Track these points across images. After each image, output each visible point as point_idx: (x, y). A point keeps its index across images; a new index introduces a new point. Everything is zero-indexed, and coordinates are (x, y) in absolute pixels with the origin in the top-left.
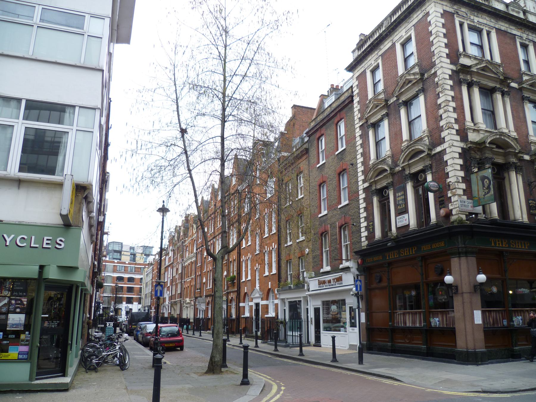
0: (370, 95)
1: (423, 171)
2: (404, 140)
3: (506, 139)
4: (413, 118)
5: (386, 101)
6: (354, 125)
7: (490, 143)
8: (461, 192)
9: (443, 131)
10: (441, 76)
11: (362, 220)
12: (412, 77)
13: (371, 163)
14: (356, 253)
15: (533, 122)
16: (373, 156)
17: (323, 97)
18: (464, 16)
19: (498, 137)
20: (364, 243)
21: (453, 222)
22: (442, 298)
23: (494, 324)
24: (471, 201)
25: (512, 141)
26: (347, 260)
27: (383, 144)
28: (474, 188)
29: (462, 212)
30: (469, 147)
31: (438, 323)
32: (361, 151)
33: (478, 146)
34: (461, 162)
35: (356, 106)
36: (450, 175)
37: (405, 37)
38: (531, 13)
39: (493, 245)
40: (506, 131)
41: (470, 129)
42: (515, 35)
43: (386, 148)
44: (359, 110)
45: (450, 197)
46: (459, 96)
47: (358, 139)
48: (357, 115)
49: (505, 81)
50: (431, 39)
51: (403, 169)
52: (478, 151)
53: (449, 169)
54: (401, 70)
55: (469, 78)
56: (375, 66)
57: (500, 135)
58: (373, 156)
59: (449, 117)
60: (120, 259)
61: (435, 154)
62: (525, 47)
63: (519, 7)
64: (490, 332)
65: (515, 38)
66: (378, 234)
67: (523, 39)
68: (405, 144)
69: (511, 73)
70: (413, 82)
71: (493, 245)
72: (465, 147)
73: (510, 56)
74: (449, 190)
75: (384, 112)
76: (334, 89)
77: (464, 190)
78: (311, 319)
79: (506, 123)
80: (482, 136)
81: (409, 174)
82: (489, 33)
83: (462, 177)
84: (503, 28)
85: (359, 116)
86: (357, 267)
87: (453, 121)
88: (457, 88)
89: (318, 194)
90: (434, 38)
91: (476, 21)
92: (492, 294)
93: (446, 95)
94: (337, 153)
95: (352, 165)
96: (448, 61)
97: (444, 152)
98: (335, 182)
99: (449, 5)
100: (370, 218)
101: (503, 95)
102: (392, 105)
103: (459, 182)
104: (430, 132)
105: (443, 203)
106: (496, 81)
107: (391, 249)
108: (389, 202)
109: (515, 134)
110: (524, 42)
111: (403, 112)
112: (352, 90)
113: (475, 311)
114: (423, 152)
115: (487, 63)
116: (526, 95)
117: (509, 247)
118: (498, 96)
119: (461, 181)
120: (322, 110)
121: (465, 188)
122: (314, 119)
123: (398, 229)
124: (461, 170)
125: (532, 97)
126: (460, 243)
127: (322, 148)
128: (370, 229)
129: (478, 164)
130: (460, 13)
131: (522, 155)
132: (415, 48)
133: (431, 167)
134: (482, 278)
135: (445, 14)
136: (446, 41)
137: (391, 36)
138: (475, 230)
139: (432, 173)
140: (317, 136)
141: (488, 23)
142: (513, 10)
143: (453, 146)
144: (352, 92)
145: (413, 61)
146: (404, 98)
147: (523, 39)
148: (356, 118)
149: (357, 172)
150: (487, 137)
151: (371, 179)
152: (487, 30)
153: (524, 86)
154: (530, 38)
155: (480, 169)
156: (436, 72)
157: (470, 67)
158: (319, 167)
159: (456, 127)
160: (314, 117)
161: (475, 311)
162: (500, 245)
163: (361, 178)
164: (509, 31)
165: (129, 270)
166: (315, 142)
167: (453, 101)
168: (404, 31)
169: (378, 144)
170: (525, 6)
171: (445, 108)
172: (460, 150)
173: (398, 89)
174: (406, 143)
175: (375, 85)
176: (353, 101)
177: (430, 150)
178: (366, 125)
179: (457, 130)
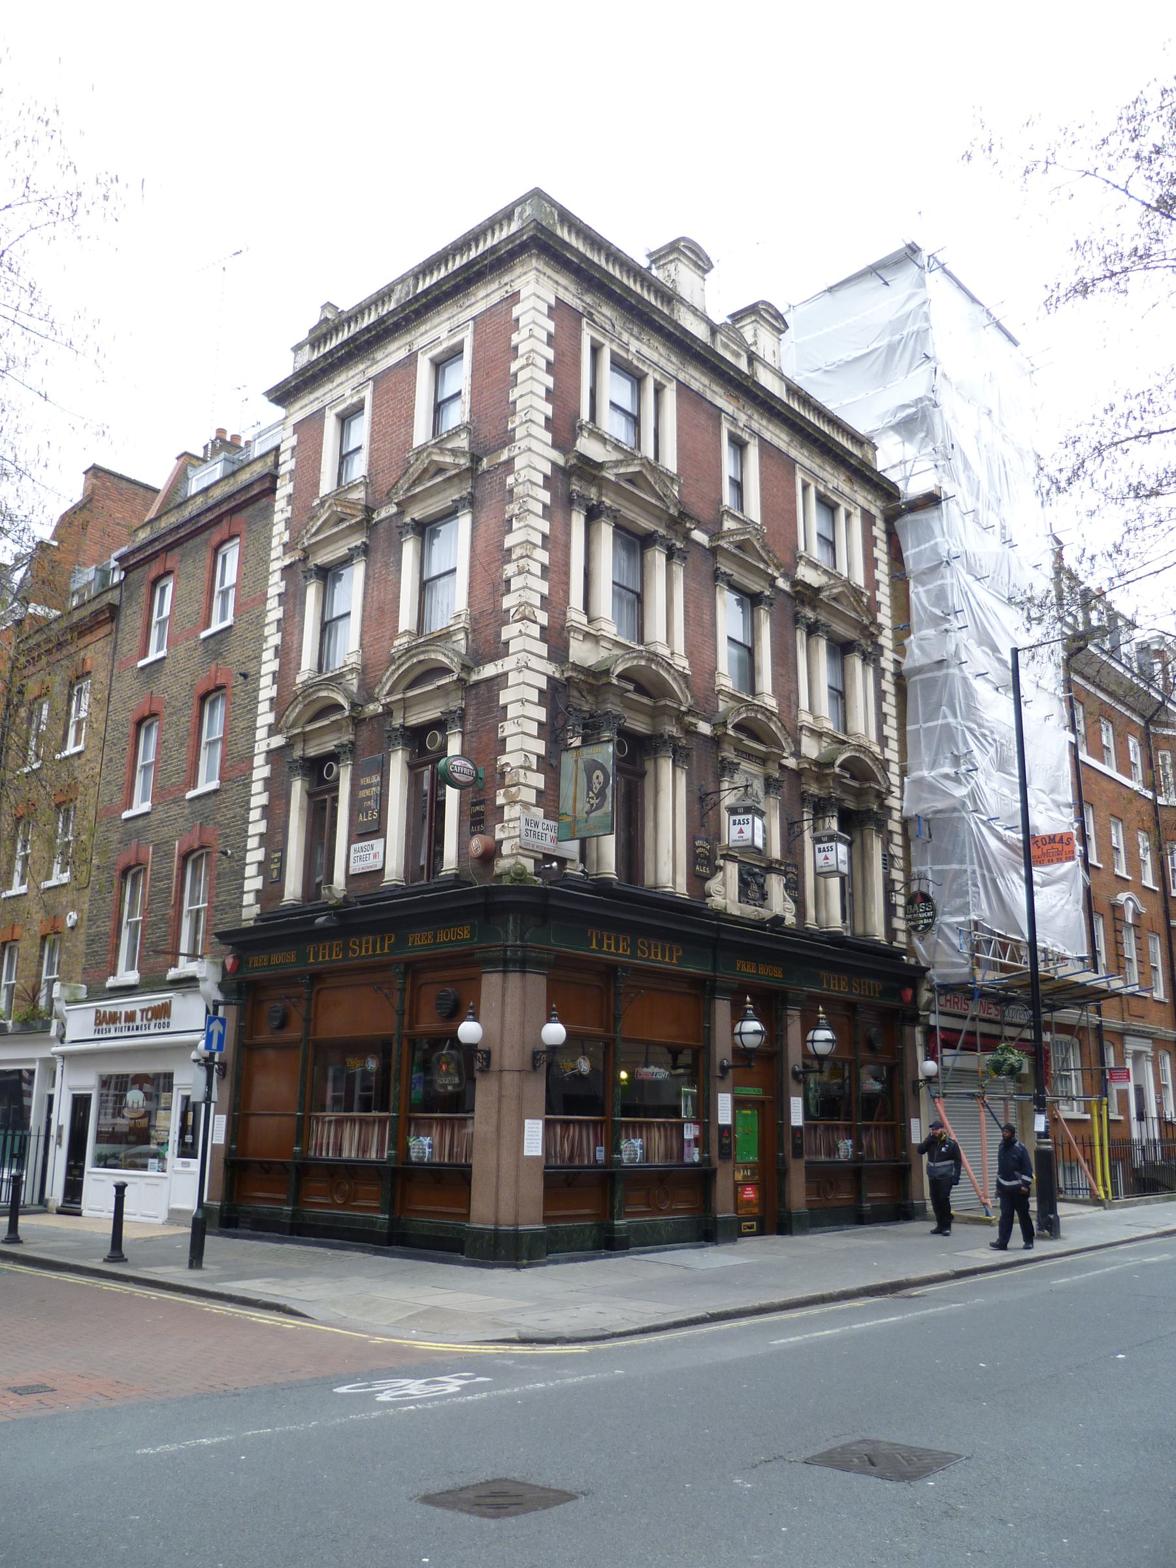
0: (327, 485)
1: (440, 725)
2: (401, 630)
3: (661, 672)
4: (434, 573)
5: (369, 510)
6: (265, 562)
7: (619, 676)
8: (530, 796)
9: (506, 623)
10: (524, 475)
11: (252, 843)
12: (448, 459)
13: (300, 679)
14: (222, 936)
15: (730, 638)
16: (308, 660)
17: (188, 461)
18: (608, 327)
19: (643, 663)
20: (250, 909)
21: (500, 876)
22: (447, 1082)
24: (552, 823)
25: (675, 679)
26: (193, 956)
27: (341, 633)
28: (567, 788)
29: (525, 851)
30: (568, 679)
32: (275, 640)
33: (591, 680)
34: (541, 714)
35: (281, 509)
36: (510, 745)
37: (445, 345)
38: (766, 365)
39: (594, 946)
40: (664, 651)
41: (577, 630)
42: (721, 410)
43: (348, 644)
44: (287, 520)
45: (502, 807)
47: (273, 603)
48: (279, 533)
49: (679, 521)
50: (514, 366)
51: (388, 712)
52: (589, 692)
53: (508, 729)
54: (421, 434)
55: (593, 493)
56: (353, 405)
57: (649, 660)
58: (308, 660)
59: (527, 588)
61: (478, 684)
62: (739, 445)
63: (741, 341)
64: (560, 1180)
65: (720, 416)
66: (293, 888)
67: (737, 426)
68: (401, 642)
69: (698, 507)
70: (449, 474)
71: (594, 946)
72: (557, 675)
73: (699, 460)
74: (502, 786)
75: (357, 540)
76: (224, 444)
77: (539, 792)
78: (60, 1128)
79: (668, 633)
80: (604, 654)
81: (402, 726)
82: (659, 390)
83: (539, 756)
84: (695, 386)
85: (286, 537)
86: (220, 980)
87: (537, 601)
88: (559, 515)
89: (129, 749)
90: (522, 368)
91: (633, 349)
92: (580, 1077)
93: (529, 530)
94: (204, 635)
95: (245, 676)
96: (548, 437)
97: (499, 681)
98: (186, 720)
99: (572, 288)
100: (274, 841)
101: (669, 558)
102: (381, 527)
103: (528, 768)
104: (473, 619)
105: (481, 822)
106: (659, 518)
107: (323, 934)
108: (335, 800)
109: (685, 663)
110: (739, 432)
111: (409, 550)
112: (277, 457)
114: (446, 671)
115: (643, 465)
116: (723, 569)
117: (633, 955)
118: (658, 558)
119: (535, 767)
120: (179, 500)
121: (542, 786)
122: (151, 521)
123: (350, 878)
124: (539, 737)
125: (736, 577)
126: (510, 935)
127: (160, 612)
128: (273, 871)
129: (585, 727)
130: (597, 317)
131: (694, 720)
132: (469, 381)
133: (462, 716)
134: (555, 1032)
135: (558, 310)
136: (549, 381)
137: (408, 331)
138: (552, 902)
139: (463, 734)
140: (153, 574)
141: (663, 362)
142: (726, 346)
143: (528, 668)
144: (277, 465)
145: (456, 415)
146: (417, 513)
147: (737, 426)
148: (275, 542)
149: (255, 701)
150: (617, 658)
151: (293, 726)
152: (655, 380)
153: (724, 543)
154: (755, 426)
155: (586, 742)
156: (511, 461)
157: (600, 466)
158: (142, 668)
159: (543, 618)
160: (151, 514)
162: (611, 948)
163: (266, 717)
164: (709, 395)
166: (144, 590)
167: (544, 547)
168: (447, 326)
169: (327, 627)
170: (755, 343)
171: (522, 562)
173: (404, 484)
174: (405, 639)
175: (344, 458)
176: (273, 490)
177: (467, 668)
178: (301, 567)
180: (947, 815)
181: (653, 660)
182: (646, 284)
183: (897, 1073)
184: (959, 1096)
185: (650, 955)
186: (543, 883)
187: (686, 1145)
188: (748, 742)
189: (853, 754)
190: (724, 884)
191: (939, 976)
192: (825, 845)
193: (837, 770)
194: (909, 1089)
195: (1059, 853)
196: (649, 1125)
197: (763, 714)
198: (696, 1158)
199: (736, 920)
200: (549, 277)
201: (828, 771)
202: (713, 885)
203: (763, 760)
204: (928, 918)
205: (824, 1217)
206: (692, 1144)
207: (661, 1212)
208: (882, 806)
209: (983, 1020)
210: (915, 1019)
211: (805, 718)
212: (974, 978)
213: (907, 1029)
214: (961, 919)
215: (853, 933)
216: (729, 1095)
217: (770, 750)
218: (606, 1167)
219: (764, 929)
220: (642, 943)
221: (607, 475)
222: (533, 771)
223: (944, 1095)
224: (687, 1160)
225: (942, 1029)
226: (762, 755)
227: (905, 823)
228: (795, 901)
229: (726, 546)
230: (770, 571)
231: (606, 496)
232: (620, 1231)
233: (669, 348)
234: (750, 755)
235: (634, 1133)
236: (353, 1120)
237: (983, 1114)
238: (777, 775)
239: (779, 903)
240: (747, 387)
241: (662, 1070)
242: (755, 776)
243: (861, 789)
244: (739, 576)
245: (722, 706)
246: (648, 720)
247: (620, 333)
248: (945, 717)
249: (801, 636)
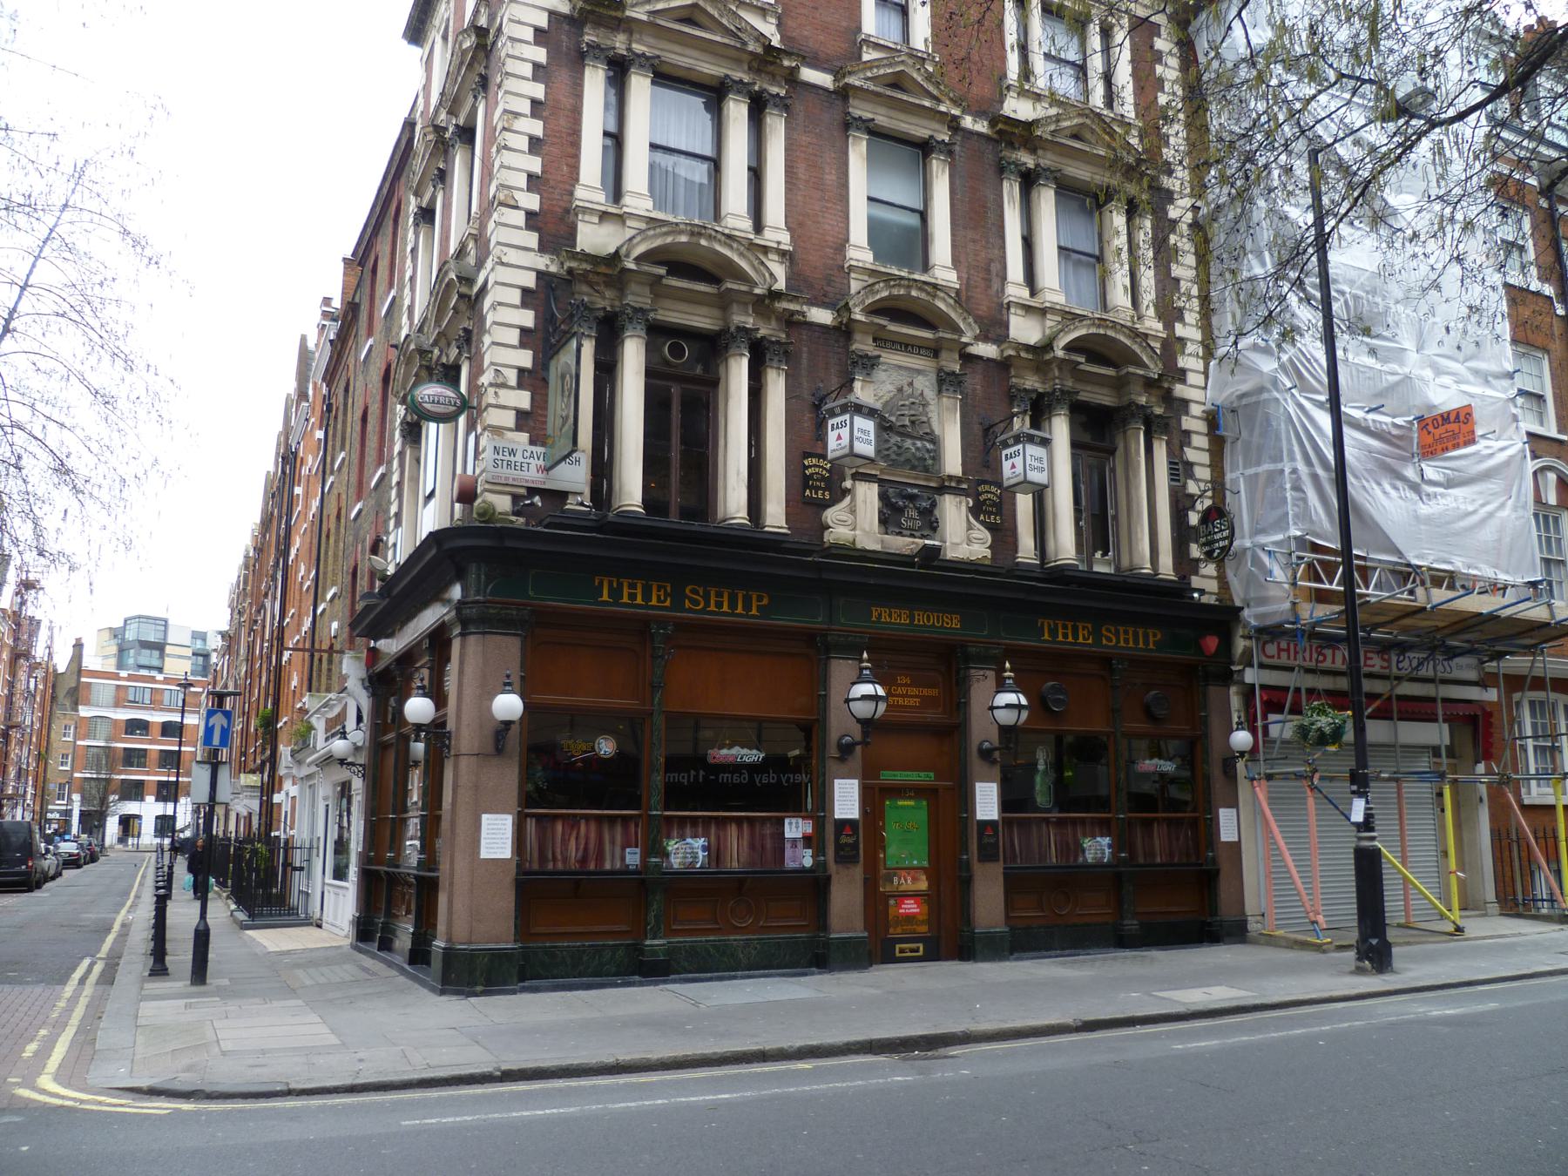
19: (684, 239)
23: (584, 860)
24: (539, 450)
25: (741, 255)
31: (701, 854)
33: (602, 269)
41: (585, 210)
46: (566, 102)
52: (607, 285)
57: (692, 234)
60: (160, 670)
64: (535, 886)
69: (812, 37)
72: (553, 269)
86: (363, 674)
88: (563, 76)
92: (597, 762)
103: (504, 386)
106: (738, 61)
113: (485, 817)
116: (857, 113)
117: (678, 605)
131: (793, 307)
143: (502, 264)
153: (854, 80)
161: (485, 817)
165: (166, 701)
172: (530, 280)
179: (530, 215)
180: (1253, 399)
181: (700, 234)
184: (1286, 776)
185: (707, 604)
186: (527, 524)
187: (788, 845)
188: (893, 327)
189: (1093, 330)
190: (853, 511)
191: (1257, 617)
192: (1012, 450)
193: (1060, 353)
194: (1216, 772)
195: (1455, 435)
196: (722, 823)
197: (920, 289)
198: (808, 862)
199: (865, 555)
201: (1048, 357)
202: (831, 515)
203: (934, 351)
204: (1223, 539)
205: (1021, 941)
206: (800, 845)
208: (1168, 398)
209: (1308, 671)
210: (1227, 677)
211: (1016, 289)
214: (1280, 537)
215: (1118, 568)
216: (856, 782)
219: (912, 565)
220: (692, 591)
222: (512, 388)
223: (1269, 777)
224: (790, 864)
225: (1263, 687)
227: (1212, 420)
228: (991, 527)
229: (857, 83)
230: (943, 108)
231: (638, 42)
232: (654, 953)
234: (906, 346)
237: (1311, 801)
238: (957, 368)
239: (961, 536)
242: (919, 372)
243: (1119, 378)
244: (883, 118)
245: (855, 286)
246: (716, 312)
249: (1011, 191)
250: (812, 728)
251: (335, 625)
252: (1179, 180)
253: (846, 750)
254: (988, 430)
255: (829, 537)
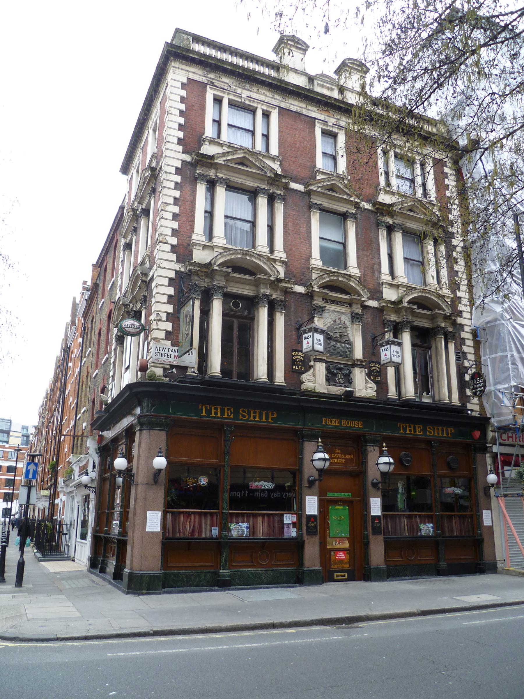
3: (254, 260)
18: (225, 88)
19: (239, 256)
24: (176, 348)
25: (264, 263)
31: (245, 530)
33: (204, 270)
41: (197, 244)
42: (315, 119)
46: (189, 198)
52: (206, 276)
57: (243, 254)
60: (7, 442)
64: (171, 545)
65: (315, 122)
67: (327, 125)
69: (294, 170)
72: (183, 269)
84: (294, 108)
86: (96, 446)
88: (187, 188)
92: (199, 488)
103: (160, 320)
106: (263, 180)
110: (331, 129)
113: (148, 512)
115: (245, 153)
116: (315, 201)
117: (236, 417)
119: (165, 319)
130: (216, 83)
131: (287, 285)
141: (268, 100)
142: (322, 86)
143: (161, 267)
147: (327, 125)
152: (263, 110)
153: (313, 188)
164: (305, 112)
165: (9, 457)
172: (172, 275)
179: (173, 246)
180: (493, 324)
181: (246, 254)
182: (259, 63)
183: (471, 481)
184: (513, 495)
185: (249, 417)
186: (170, 381)
187: (285, 527)
188: (331, 294)
189: (420, 294)
190: (314, 375)
191: (497, 422)
192: (385, 348)
193: (406, 305)
194: (481, 493)
196: (255, 516)
197: (343, 277)
198: (294, 534)
199: (320, 395)
200: (182, 69)
201: (400, 306)
202: (304, 377)
203: (350, 304)
204: (481, 387)
205: (392, 572)
206: (291, 526)
207: (261, 566)
208: (454, 324)
210: (485, 450)
211: (386, 277)
212: (516, 421)
213: (479, 456)
214: (507, 386)
215: (433, 400)
216: (316, 497)
217: (351, 297)
218: (218, 539)
219: (341, 399)
221: (218, 162)
222: (164, 321)
223: (505, 496)
224: (286, 535)
226: (348, 301)
227: (475, 333)
228: (376, 382)
229: (315, 189)
230: (352, 199)
231: (219, 173)
232: (224, 576)
233: (273, 92)
234: (337, 302)
235: (234, 520)
236: (263, 515)
239: (363, 386)
240: (332, 104)
241: (270, 483)
242: (343, 313)
243: (432, 315)
244: (326, 204)
245: (314, 276)
246: (254, 288)
247: (235, 89)
248: (490, 266)
249: (382, 234)
250: (296, 473)
251: (84, 424)
252: (457, 229)
253: (311, 483)
254: (374, 339)
255: (304, 387)
